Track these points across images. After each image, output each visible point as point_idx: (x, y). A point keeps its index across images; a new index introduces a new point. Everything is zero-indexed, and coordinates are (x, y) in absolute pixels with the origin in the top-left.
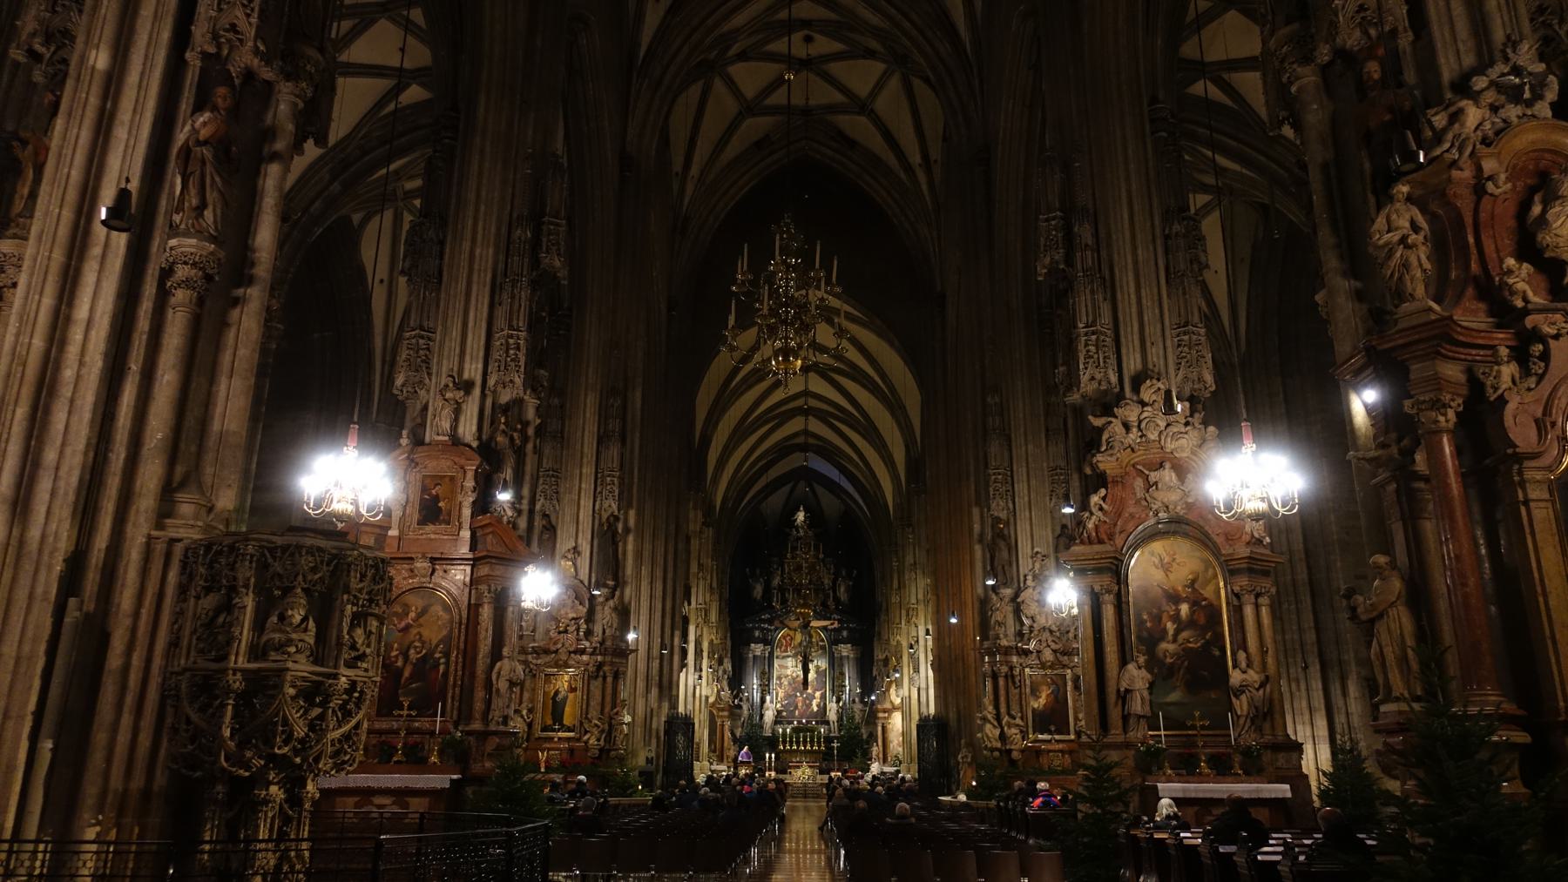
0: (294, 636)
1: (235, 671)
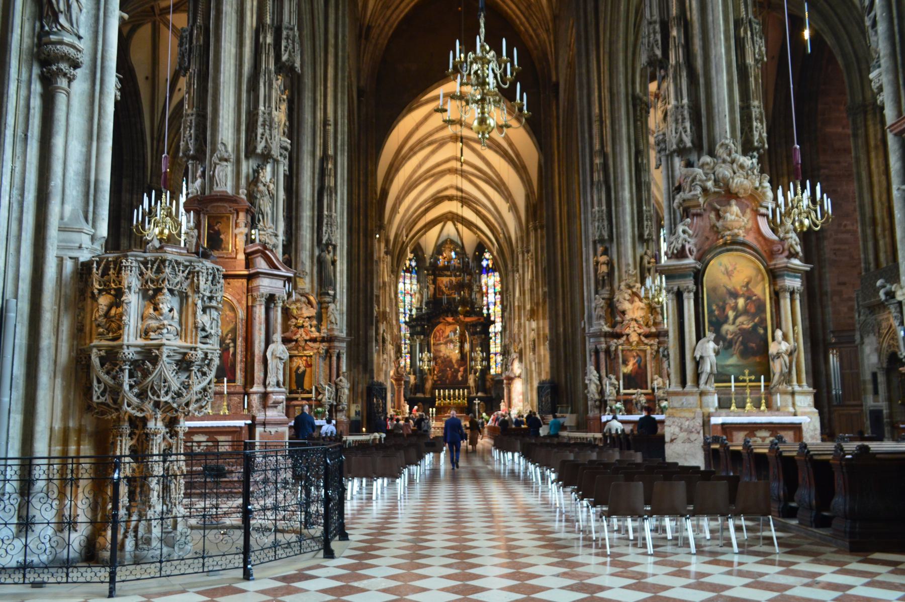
0: (166, 322)
1: (128, 346)
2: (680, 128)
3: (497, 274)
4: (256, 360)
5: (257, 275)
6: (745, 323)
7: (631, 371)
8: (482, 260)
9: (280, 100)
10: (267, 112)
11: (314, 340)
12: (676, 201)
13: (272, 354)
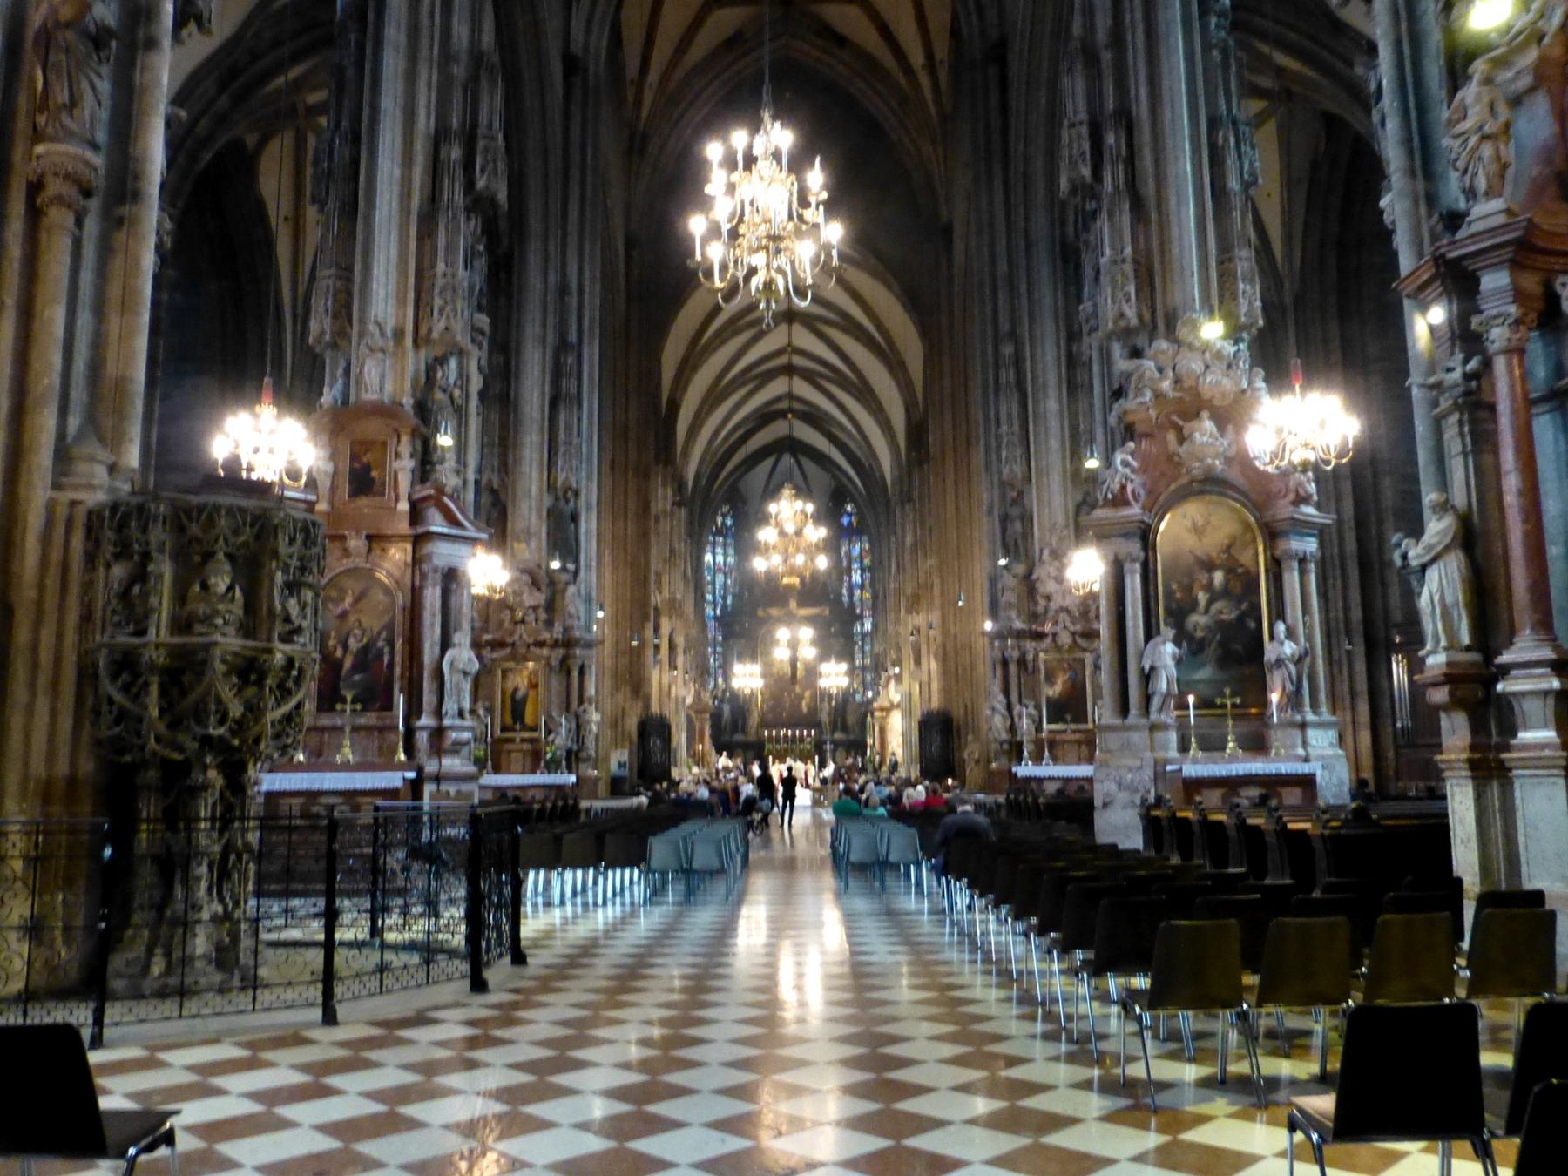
0: (221, 607)
1: (157, 646)
2: (1120, 295)
3: (865, 538)
4: (426, 675)
5: (429, 536)
6: (1226, 611)
7: (1061, 694)
8: (841, 516)
9: (473, 254)
10: (449, 271)
11: (541, 644)
12: (1114, 413)
13: (452, 664)
